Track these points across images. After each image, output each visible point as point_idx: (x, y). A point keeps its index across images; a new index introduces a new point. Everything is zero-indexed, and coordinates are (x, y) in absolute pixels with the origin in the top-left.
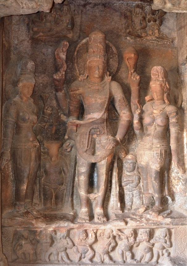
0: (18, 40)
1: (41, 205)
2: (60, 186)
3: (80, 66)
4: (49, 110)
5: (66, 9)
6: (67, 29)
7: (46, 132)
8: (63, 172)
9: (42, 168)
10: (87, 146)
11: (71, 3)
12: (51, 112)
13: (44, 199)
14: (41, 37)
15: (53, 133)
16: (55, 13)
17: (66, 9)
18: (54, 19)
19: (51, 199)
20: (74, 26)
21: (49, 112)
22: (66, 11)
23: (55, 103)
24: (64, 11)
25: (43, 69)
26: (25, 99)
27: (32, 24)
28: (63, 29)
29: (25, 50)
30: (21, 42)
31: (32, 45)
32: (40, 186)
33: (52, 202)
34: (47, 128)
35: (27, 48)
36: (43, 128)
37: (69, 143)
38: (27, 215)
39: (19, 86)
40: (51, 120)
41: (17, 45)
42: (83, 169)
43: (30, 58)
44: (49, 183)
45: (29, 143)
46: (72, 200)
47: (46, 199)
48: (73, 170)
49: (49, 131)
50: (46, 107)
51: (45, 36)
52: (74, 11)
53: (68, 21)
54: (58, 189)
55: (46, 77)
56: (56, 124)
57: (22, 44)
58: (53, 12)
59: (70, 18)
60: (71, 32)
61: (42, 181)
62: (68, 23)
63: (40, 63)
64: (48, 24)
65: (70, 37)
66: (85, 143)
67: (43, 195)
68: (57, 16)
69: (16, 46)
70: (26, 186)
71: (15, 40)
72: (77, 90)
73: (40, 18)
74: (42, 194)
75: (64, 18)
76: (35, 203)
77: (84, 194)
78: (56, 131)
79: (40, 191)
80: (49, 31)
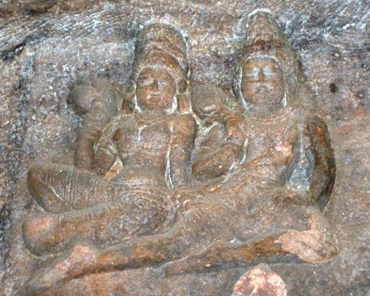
5: (268, 72)
6: (276, 200)
11: (305, 44)
14: (86, 278)
16: (189, 111)
17: (268, 72)
18: (180, 149)
20: (331, 180)
22: (269, 86)
24: (253, 87)
27: (28, 207)
28: (251, 203)
51: (121, 267)
52: (333, 88)
53: (285, 151)
58: (175, 106)
59: (301, 128)
60: (309, 216)
62: (290, 163)
64: (137, 181)
65: (308, 254)
68: (204, 131)
73: (83, 153)
75: (251, 135)
80: (147, 229)
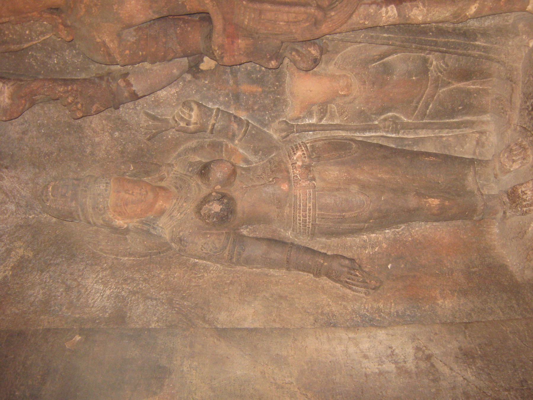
0: (5, 203)
1: (483, 122)
2: (432, 68)
3: (27, 32)
4: (190, 116)
7: (258, 109)
8: (386, 59)
9: (371, 123)
10: (303, 9)
12: (195, 107)
13: (467, 114)
15: (260, 90)
19: (469, 93)
21: (194, 116)
23: (165, 93)
25: (69, 133)
26: (161, 203)
29: (27, 184)
30: (7, 195)
31: (7, 168)
32: (425, 126)
33: (478, 91)
34: (247, 110)
35: (19, 178)
36: (246, 132)
37: (294, 53)
38: (524, 203)
39: (126, 226)
40: (221, 99)
41: (18, 205)
42: (387, 12)
43: (44, 169)
44: (418, 103)
45: (295, 196)
46: (485, 33)
47: (468, 109)
48: (385, 35)
49: (255, 103)
50: (182, 124)
54: (439, 74)
55: (91, 123)
56: (231, 82)
57: (11, 192)
61: (410, 121)
63: (55, 141)
66: (294, 15)
67: (453, 118)
69: (21, 207)
70: (430, 200)
71: (7, 211)
72: (108, 48)
74: (452, 120)
76: (478, 143)
77: (477, 5)
78: (254, 82)
79: (442, 127)
